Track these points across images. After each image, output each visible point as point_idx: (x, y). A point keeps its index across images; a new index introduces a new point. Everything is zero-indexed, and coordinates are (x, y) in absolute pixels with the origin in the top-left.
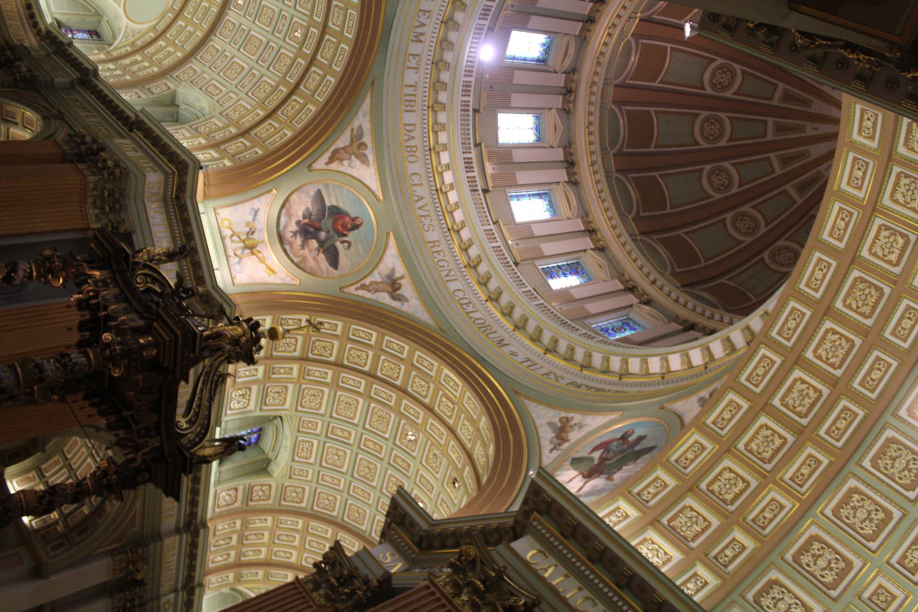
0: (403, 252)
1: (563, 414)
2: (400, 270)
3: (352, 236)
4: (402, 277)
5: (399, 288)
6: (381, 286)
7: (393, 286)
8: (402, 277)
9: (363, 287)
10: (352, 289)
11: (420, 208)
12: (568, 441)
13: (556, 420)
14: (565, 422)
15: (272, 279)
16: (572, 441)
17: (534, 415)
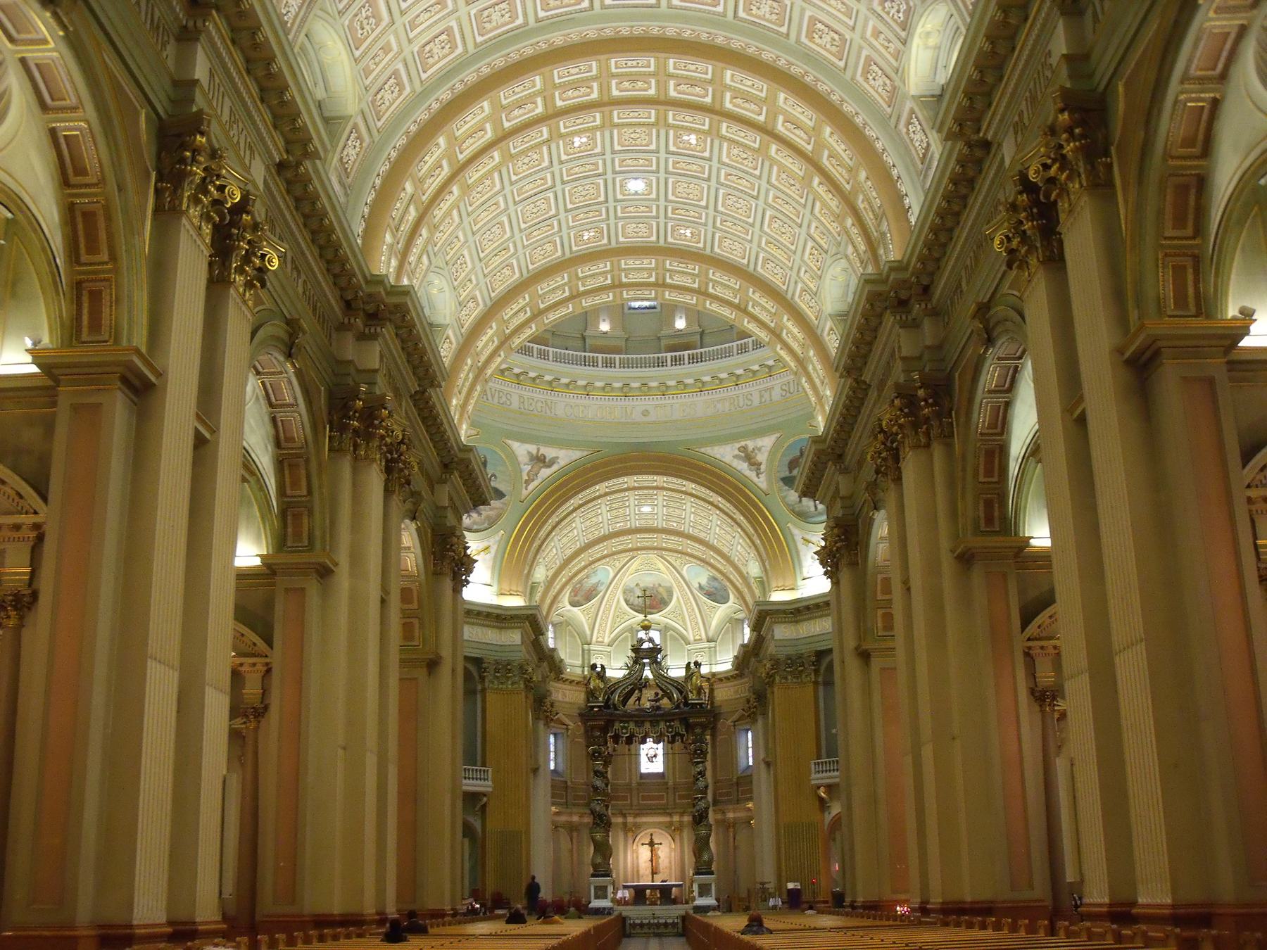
0: (523, 439)
1: (737, 445)
2: (532, 448)
3: (490, 471)
4: (538, 450)
5: (545, 457)
6: (535, 469)
7: (540, 460)
8: (538, 450)
9: (527, 482)
10: (525, 493)
11: (493, 397)
12: (760, 464)
13: (737, 452)
14: (744, 449)
15: (493, 550)
16: (764, 462)
17: (718, 456)
